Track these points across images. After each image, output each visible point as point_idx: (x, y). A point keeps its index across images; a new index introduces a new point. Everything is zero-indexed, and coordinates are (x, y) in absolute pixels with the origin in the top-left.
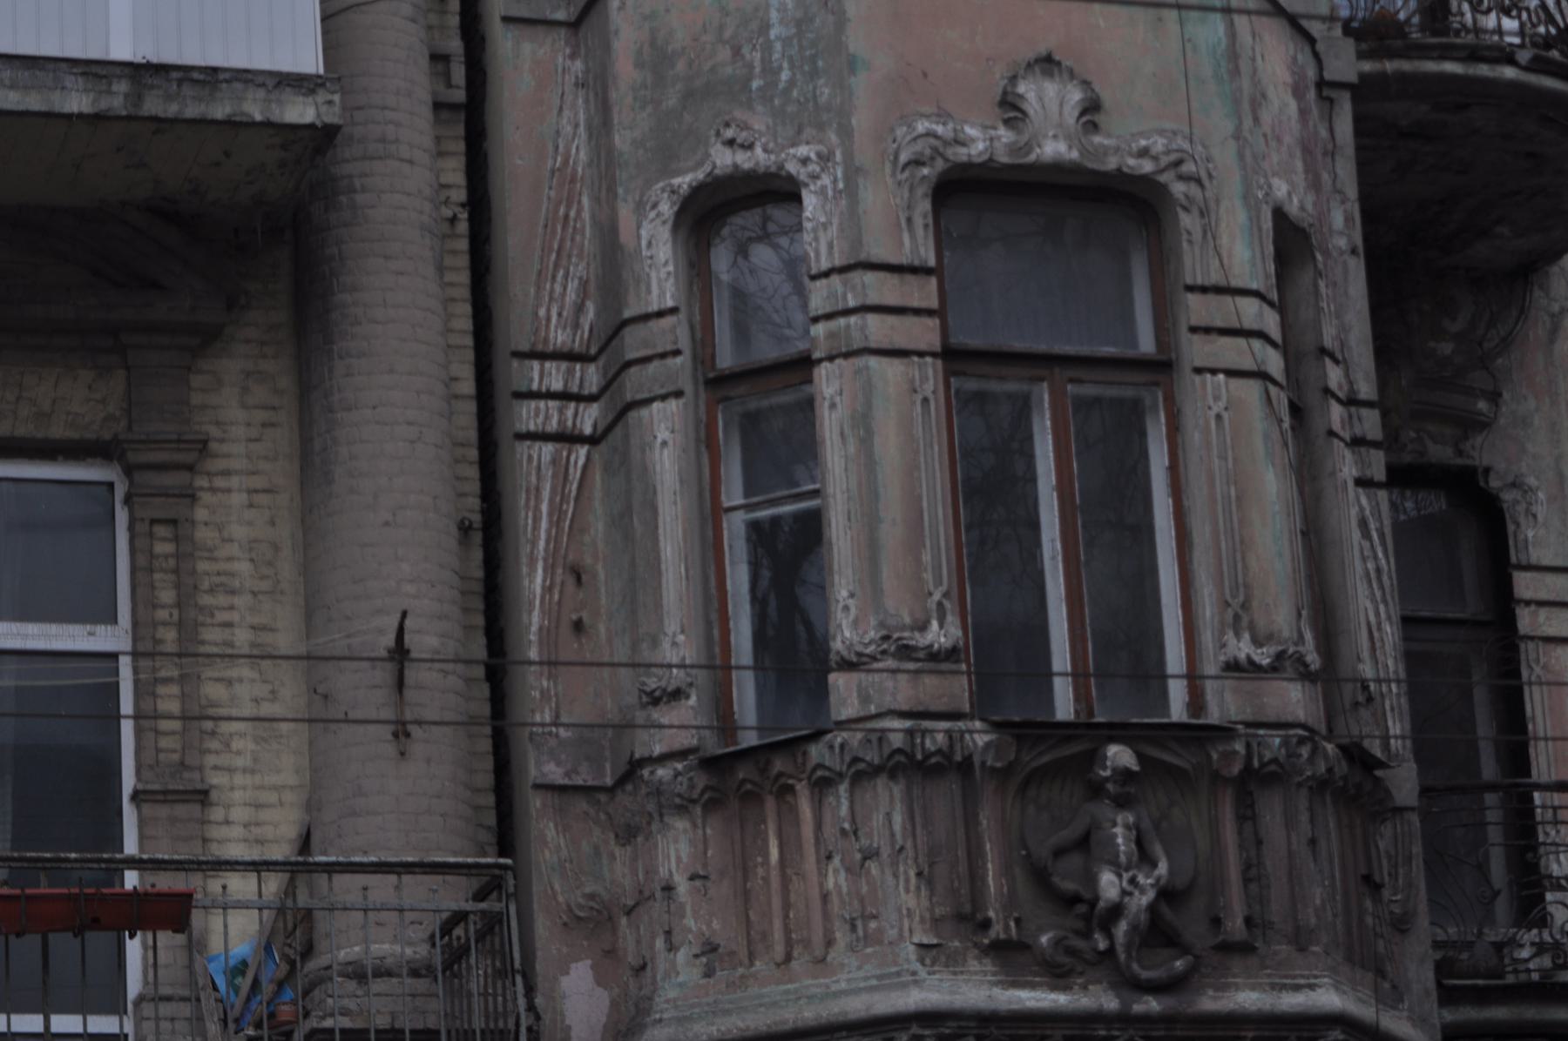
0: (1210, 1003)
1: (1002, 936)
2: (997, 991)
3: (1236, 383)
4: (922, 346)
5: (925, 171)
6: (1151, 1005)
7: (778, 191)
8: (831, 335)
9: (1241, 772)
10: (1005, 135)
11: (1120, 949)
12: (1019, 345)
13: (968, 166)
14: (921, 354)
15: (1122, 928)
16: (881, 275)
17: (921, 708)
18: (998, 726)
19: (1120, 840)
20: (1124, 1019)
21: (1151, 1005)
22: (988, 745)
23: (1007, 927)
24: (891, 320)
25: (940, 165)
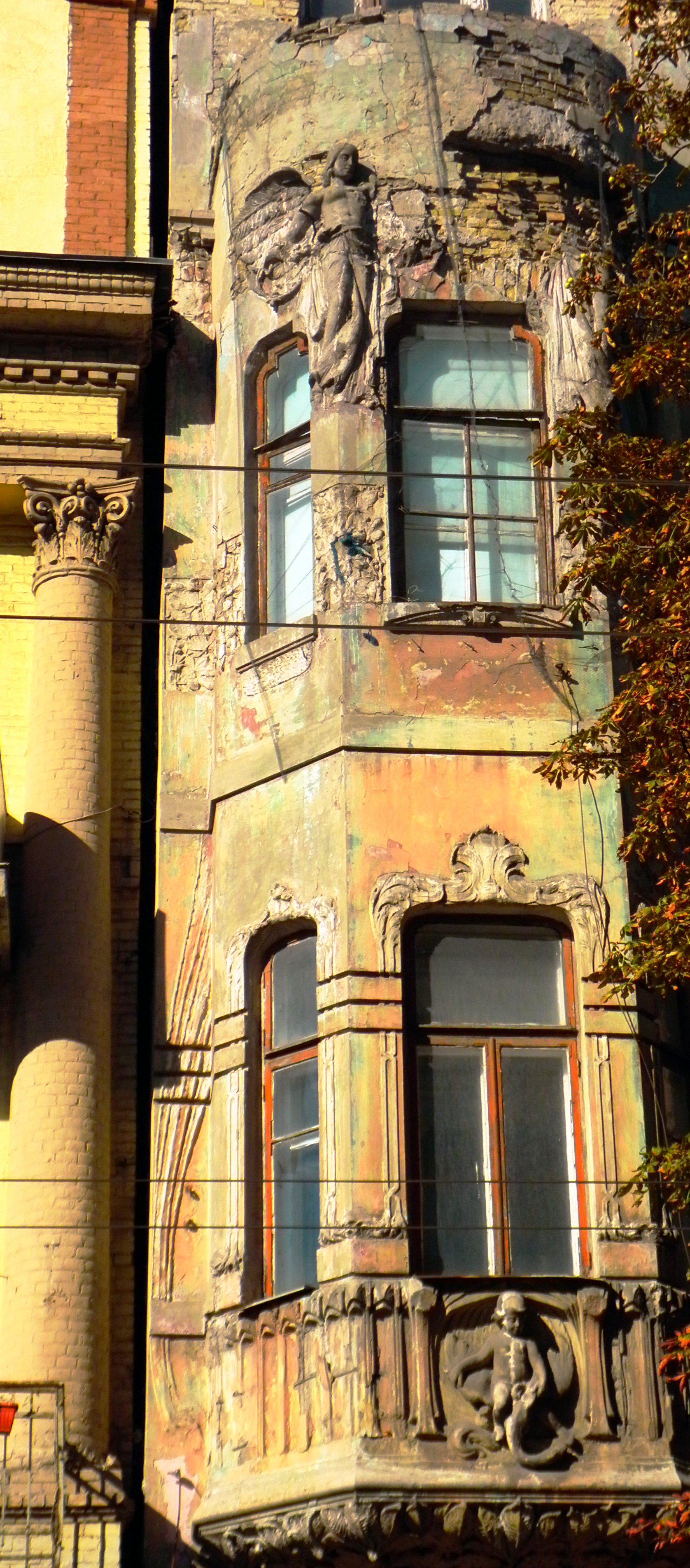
0: (578, 1477)
1: (424, 1430)
2: (418, 1471)
3: (616, 1043)
4: (389, 1025)
5: (394, 909)
6: (536, 1480)
7: (305, 928)
8: (329, 1019)
9: (605, 1312)
10: (455, 882)
11: (509, 1439)
12: (465, 1025)
13: (428, 905)
14: (388, 1031)
15: (510, 1422)
16: (362, 978)
17: (373, 1271)
18: (426, 1282)
19: (511, 1361)
20: (514, 1491)
21: (536, 1480)
22: (416, 1295)
23: (428, 1424)
24: (367, 1008)
25: (407, 905)
